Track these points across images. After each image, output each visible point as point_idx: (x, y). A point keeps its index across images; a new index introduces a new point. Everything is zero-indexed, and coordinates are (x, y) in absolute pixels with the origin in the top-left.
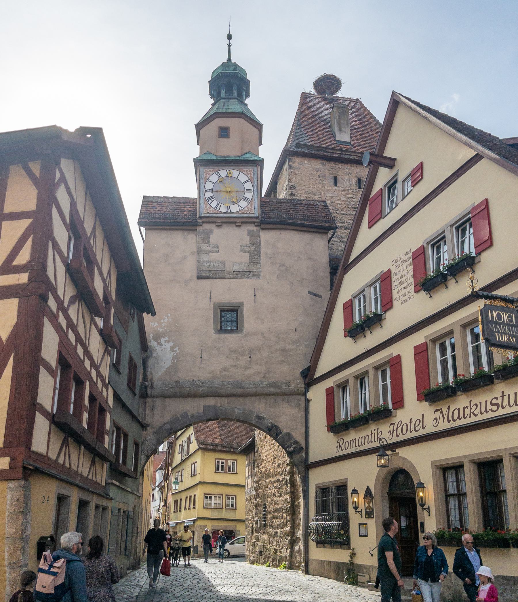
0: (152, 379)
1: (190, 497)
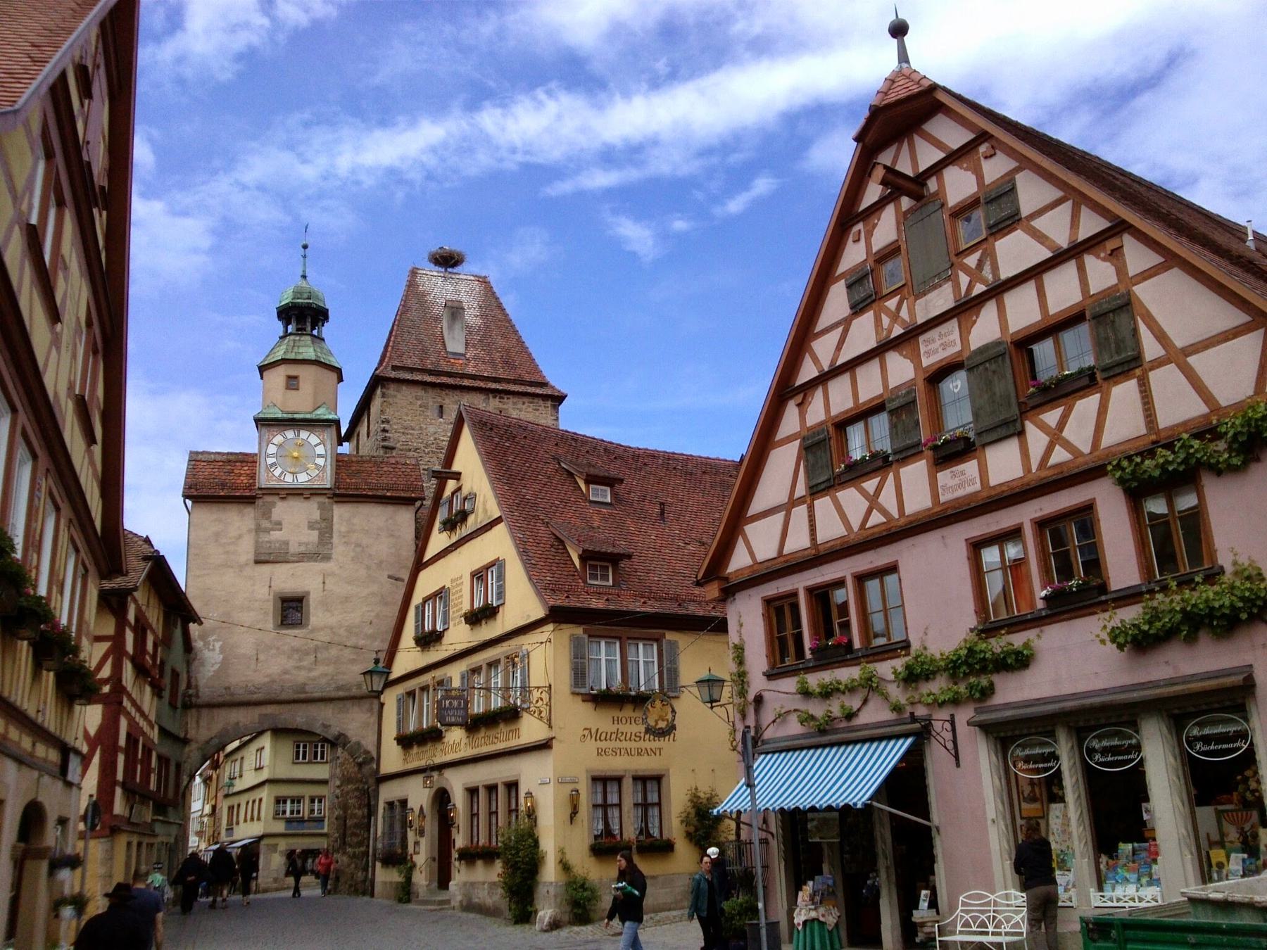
0: (197, 687)
1: (254, 801)
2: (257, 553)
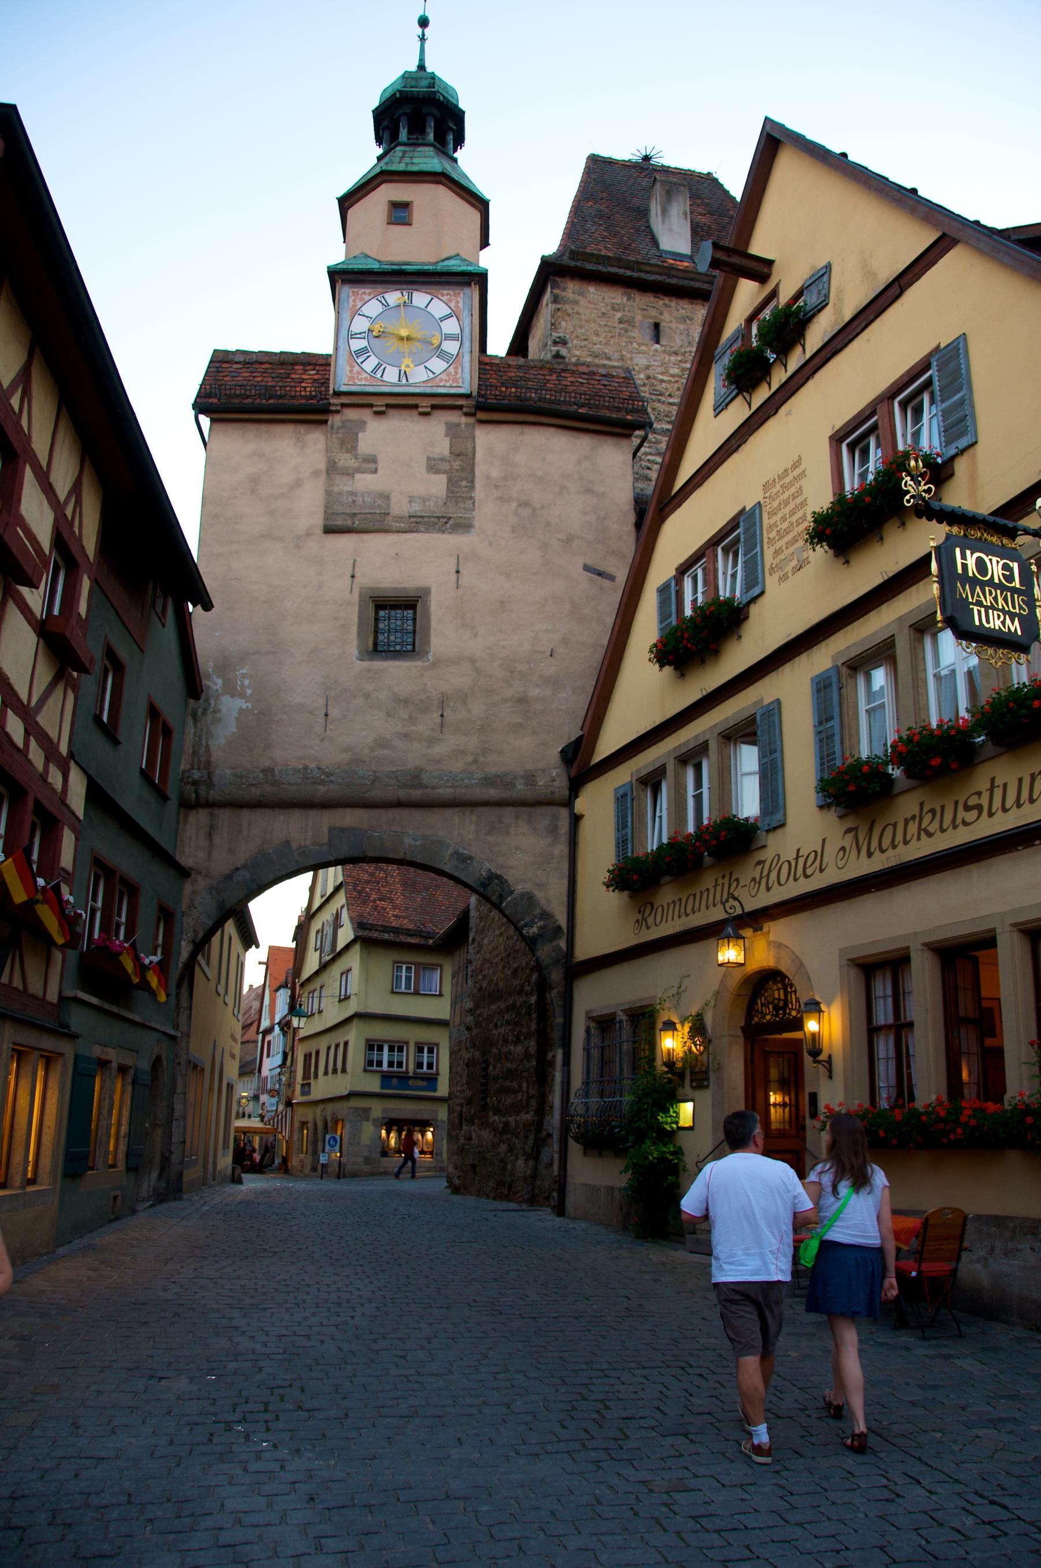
1: (337, 1046)
2: (329, 512)
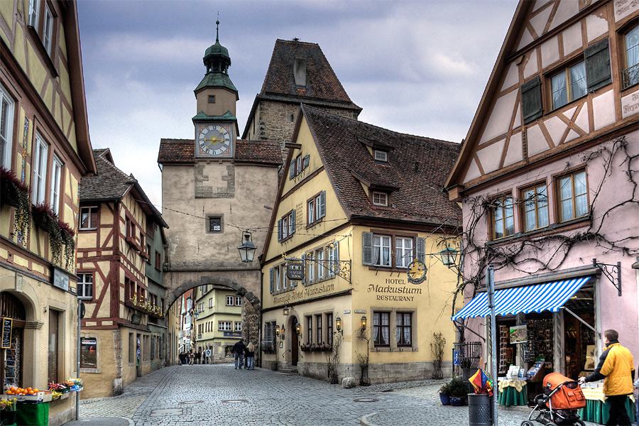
2: (196, 193)
